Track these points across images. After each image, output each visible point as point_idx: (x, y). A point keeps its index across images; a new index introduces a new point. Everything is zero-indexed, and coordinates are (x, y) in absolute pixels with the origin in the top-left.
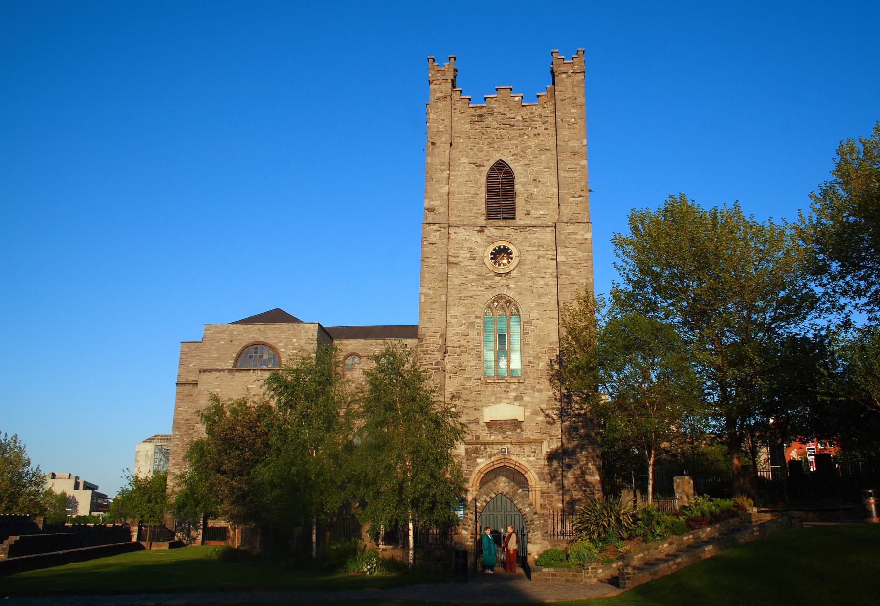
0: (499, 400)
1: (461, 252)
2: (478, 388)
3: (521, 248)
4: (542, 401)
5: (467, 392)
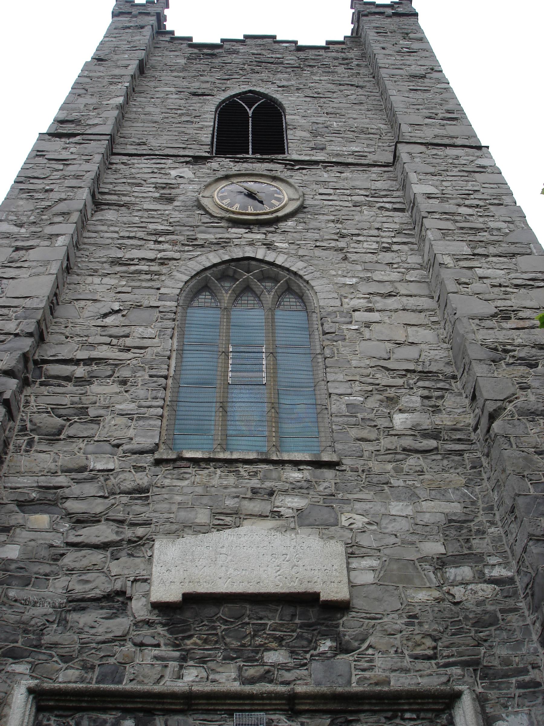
0: (225, 519)
1: (137, 189)
2: (142, 479)
3: (306, 190)
4: (420, 531)
5: (90, 489)
